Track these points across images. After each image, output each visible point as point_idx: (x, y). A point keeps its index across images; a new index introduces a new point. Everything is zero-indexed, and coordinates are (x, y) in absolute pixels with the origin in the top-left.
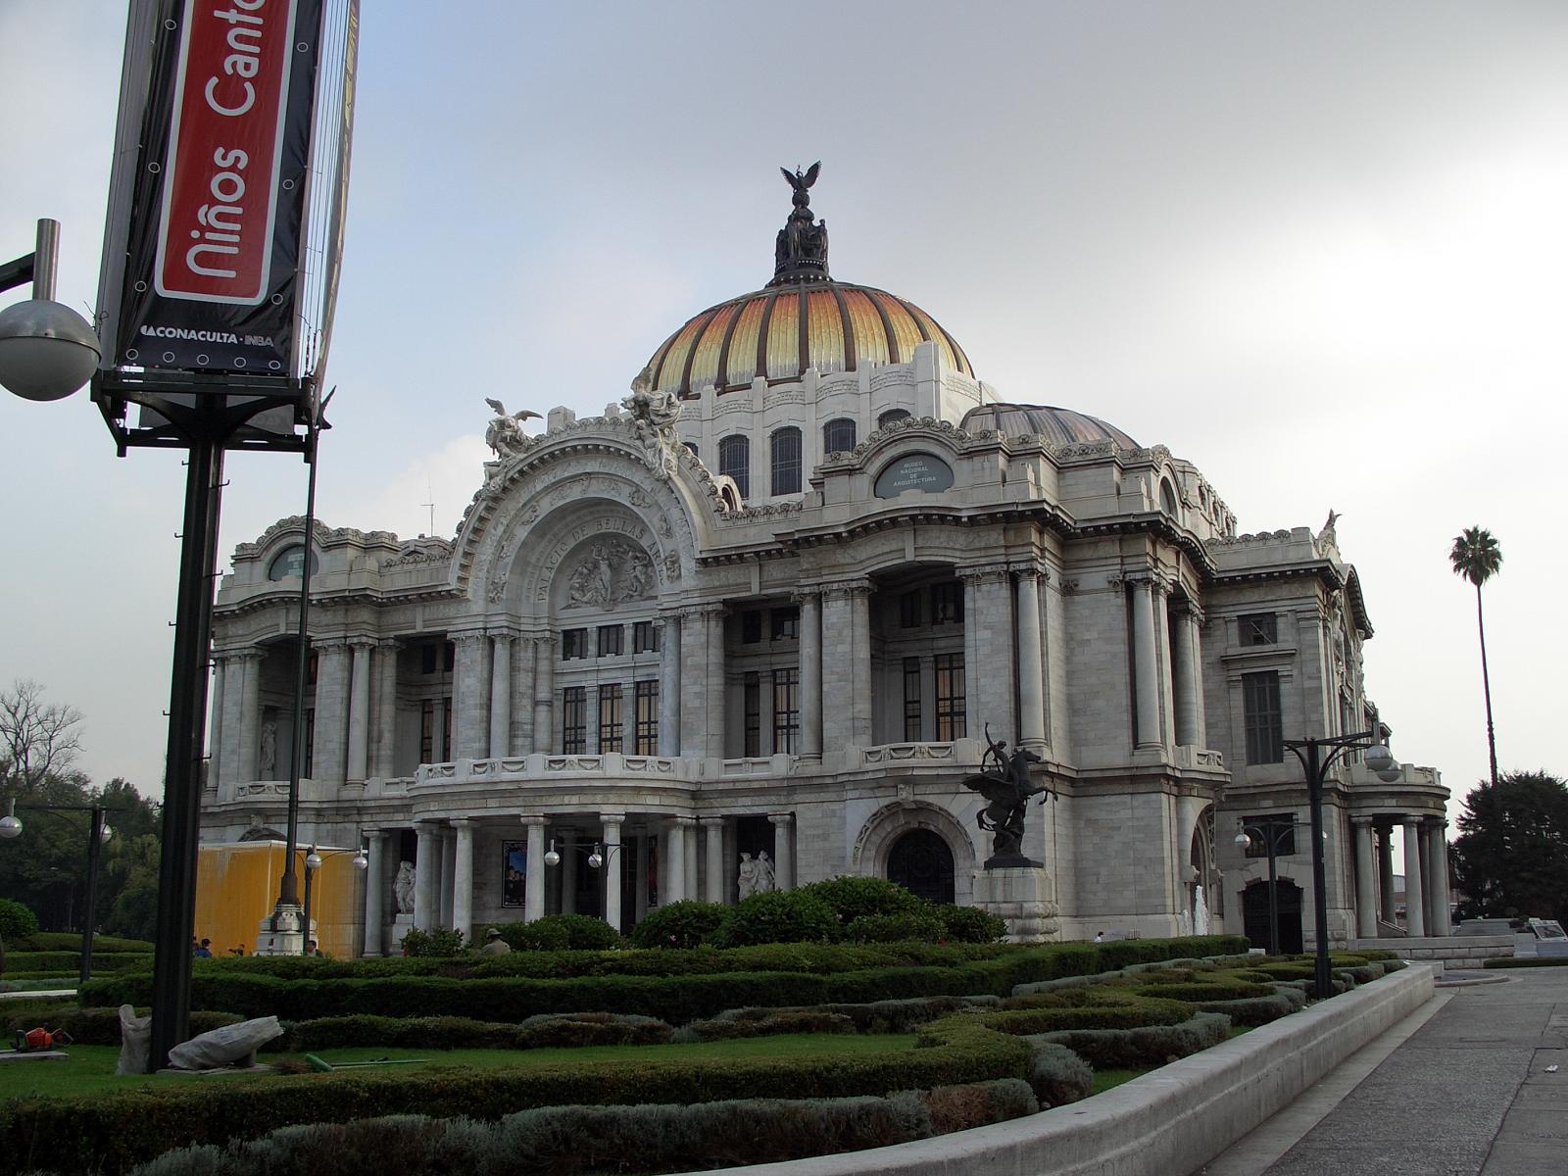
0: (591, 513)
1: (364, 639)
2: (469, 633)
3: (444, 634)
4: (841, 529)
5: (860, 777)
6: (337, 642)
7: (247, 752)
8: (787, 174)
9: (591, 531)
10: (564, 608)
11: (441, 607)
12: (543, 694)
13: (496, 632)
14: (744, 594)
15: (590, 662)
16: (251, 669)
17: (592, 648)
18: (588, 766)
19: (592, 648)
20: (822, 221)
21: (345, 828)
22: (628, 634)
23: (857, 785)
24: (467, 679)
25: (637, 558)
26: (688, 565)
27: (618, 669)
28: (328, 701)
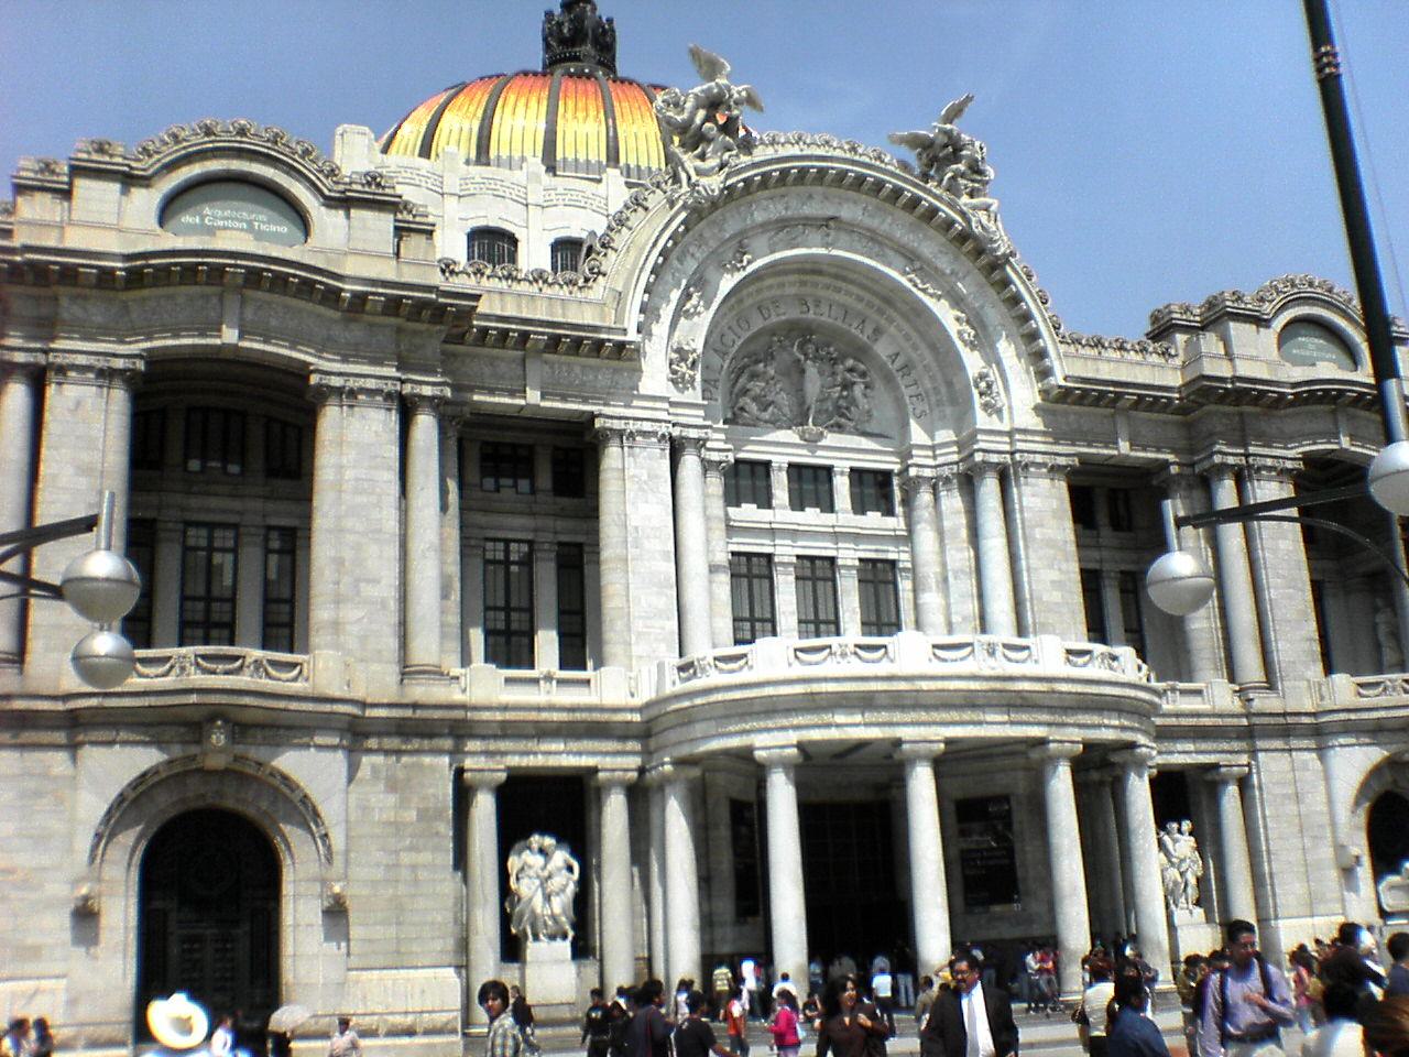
0: (803, 283)
1: (448, 392)
5: (1365, 716)
6: (390, 387)
9: (793, 313)
11: (577, 370)
12: (722, 558)
13: (693, 434)
17: (781, 493)
18: (1115, 664)
19: (781, 493)
20: (610, 21)
21: (421, 766)
22: (842, 485)
23: (1349, 728)
25: (851, 370)
26: (1021, 400)
27: (845, 532)
28: (362, 499)
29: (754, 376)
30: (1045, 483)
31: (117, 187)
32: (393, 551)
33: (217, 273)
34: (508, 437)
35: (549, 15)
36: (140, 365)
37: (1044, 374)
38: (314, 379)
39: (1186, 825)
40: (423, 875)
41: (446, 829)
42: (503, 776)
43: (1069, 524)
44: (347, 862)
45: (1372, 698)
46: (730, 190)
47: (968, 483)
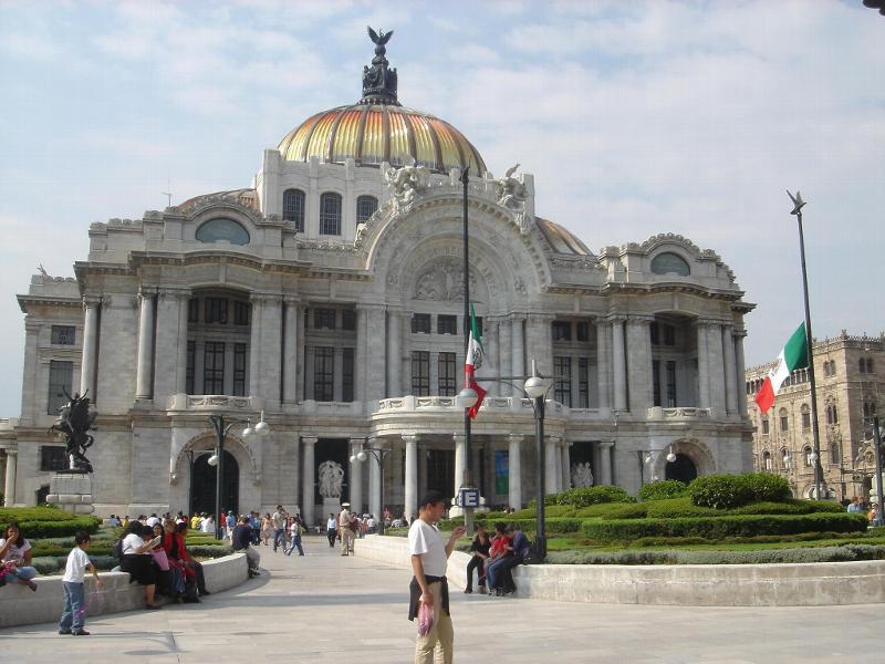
1: (299, 299)
2: (375, 307)
3: (354, 305)
4: (648, 288)
7: (181, 371)
8: (372, 34)
10: (414, 298)
12: (407, 355)
13: (395, 309)
14: (570, 312)
15: (435, 335)
16: (184, 304)
17: (434, 327)
19: (434, 327)
24: (371, 340)
26: (535, 290)
29: (426, 280)
30: (541, 326)
31: (178, 225)
32: (279, 359)
33: (217, 258)
34: (326, 307)
35: (366, 67)
36: (190, 293)
37: (544, 281)
38: (252, 296)
39: (588, 464)
40: (288, 473)
41: (296, 457)
42: (316, 441)
43: (550, 343)
44: (262, 468)
45: (670, 417)
46: (413, 210)
47: (510, 324)
